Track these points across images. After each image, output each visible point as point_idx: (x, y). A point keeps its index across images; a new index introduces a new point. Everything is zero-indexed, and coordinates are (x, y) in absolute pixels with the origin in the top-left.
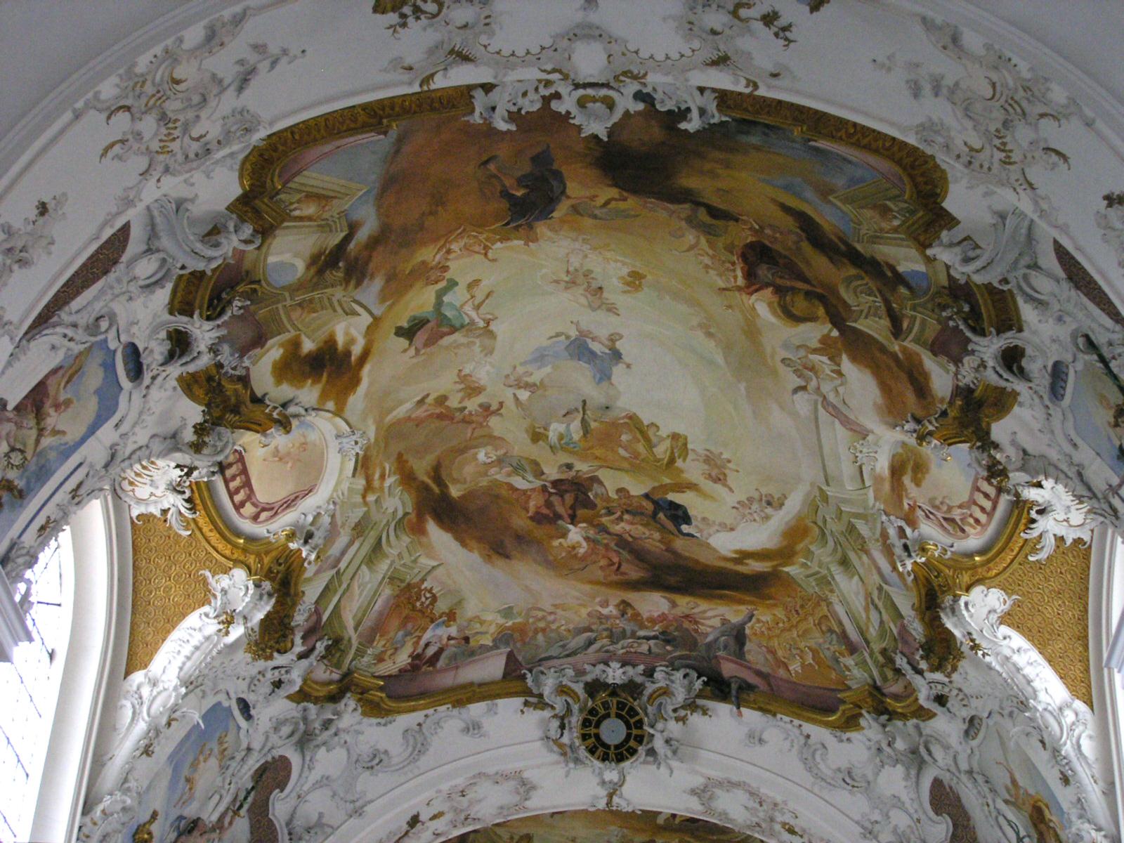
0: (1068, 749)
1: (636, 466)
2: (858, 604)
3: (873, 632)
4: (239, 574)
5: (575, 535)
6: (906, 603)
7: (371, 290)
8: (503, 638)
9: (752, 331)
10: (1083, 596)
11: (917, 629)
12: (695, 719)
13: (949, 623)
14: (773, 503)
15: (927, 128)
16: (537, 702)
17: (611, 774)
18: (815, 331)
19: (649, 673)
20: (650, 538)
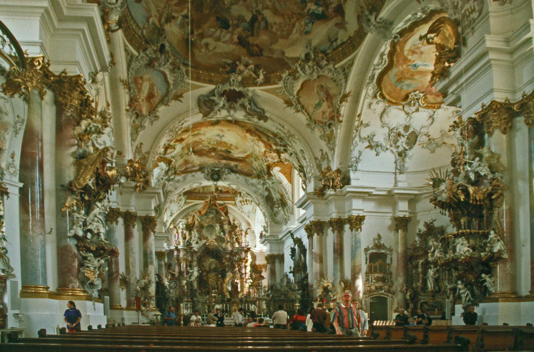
0: (287, 190)
1: (224, 147)
2: (257, 165)
3: (259, 169)
4: (162, 163)
5: (213, 154)
6: (265, 167)
7: (190, 133)
8: (199, 165)
9: (246, 136)
10: (291, 174)
11: (266, 170)
12: (229, 175)
13: (271, 172)
14: (245, 152)
15: (278, 133)
16: (204, 172)
17: (215, 183)
18: (255, 138)
19: (222, 169)
20: (225, 154)
